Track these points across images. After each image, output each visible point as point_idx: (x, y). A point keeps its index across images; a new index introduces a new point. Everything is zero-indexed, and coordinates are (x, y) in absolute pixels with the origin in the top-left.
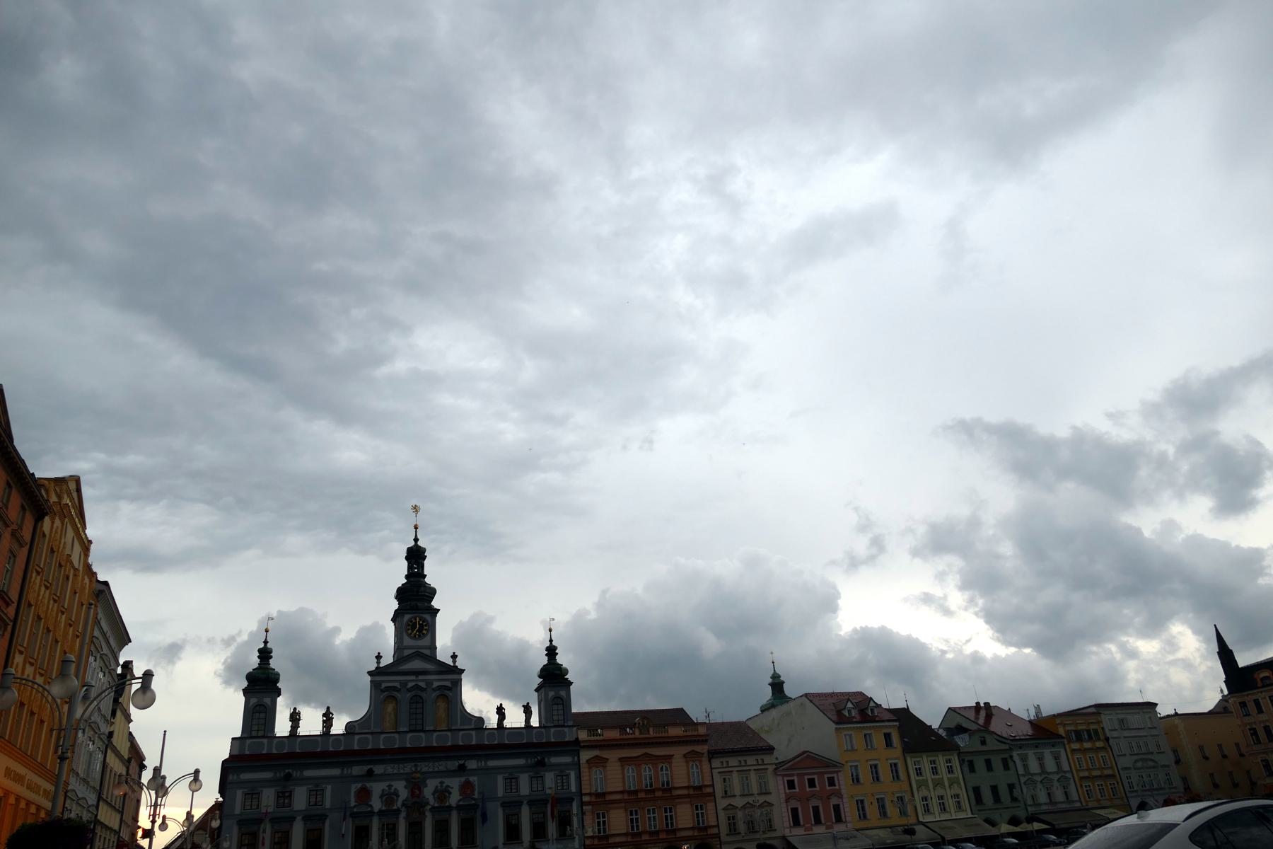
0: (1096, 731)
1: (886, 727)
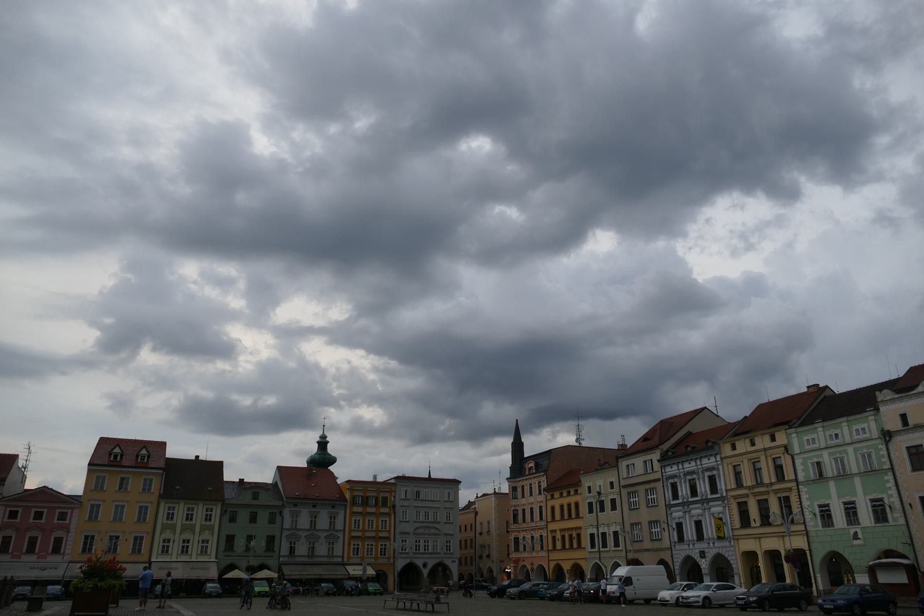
0: (385, 499)
1: (147, 474)
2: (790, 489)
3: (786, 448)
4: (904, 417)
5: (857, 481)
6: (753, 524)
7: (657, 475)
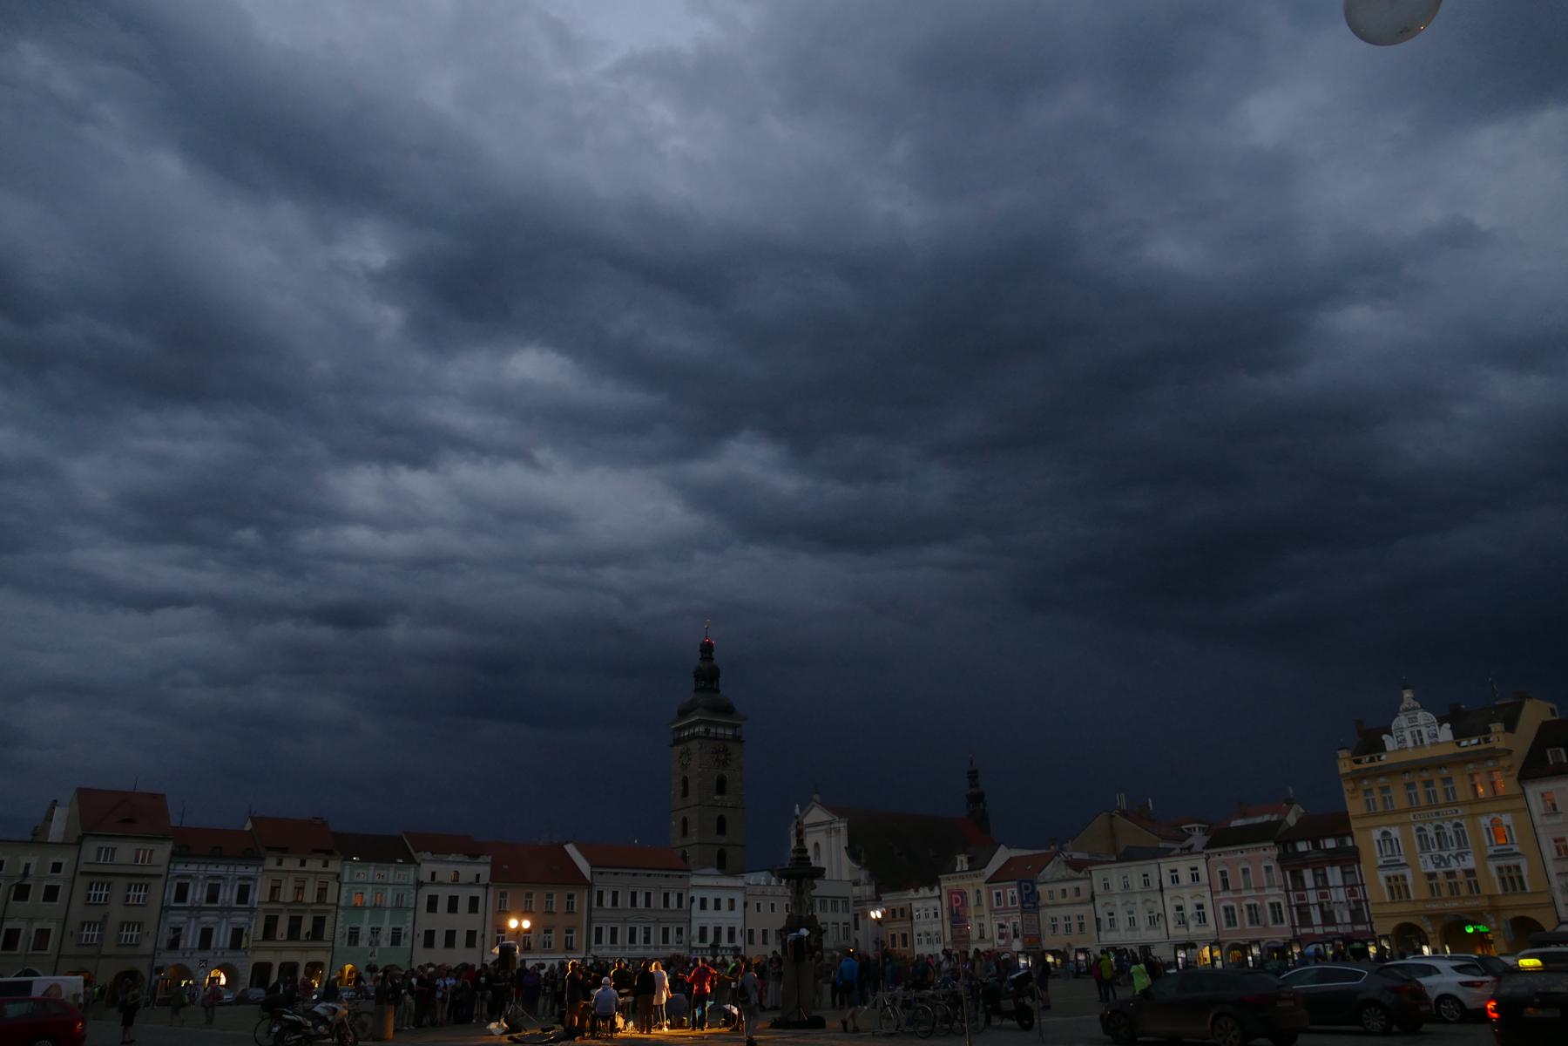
2: (328, 911)
3: (338, 876)
4: (433, 874)
5: (388, 913)
6: (278, 937)
7: (162, 870)
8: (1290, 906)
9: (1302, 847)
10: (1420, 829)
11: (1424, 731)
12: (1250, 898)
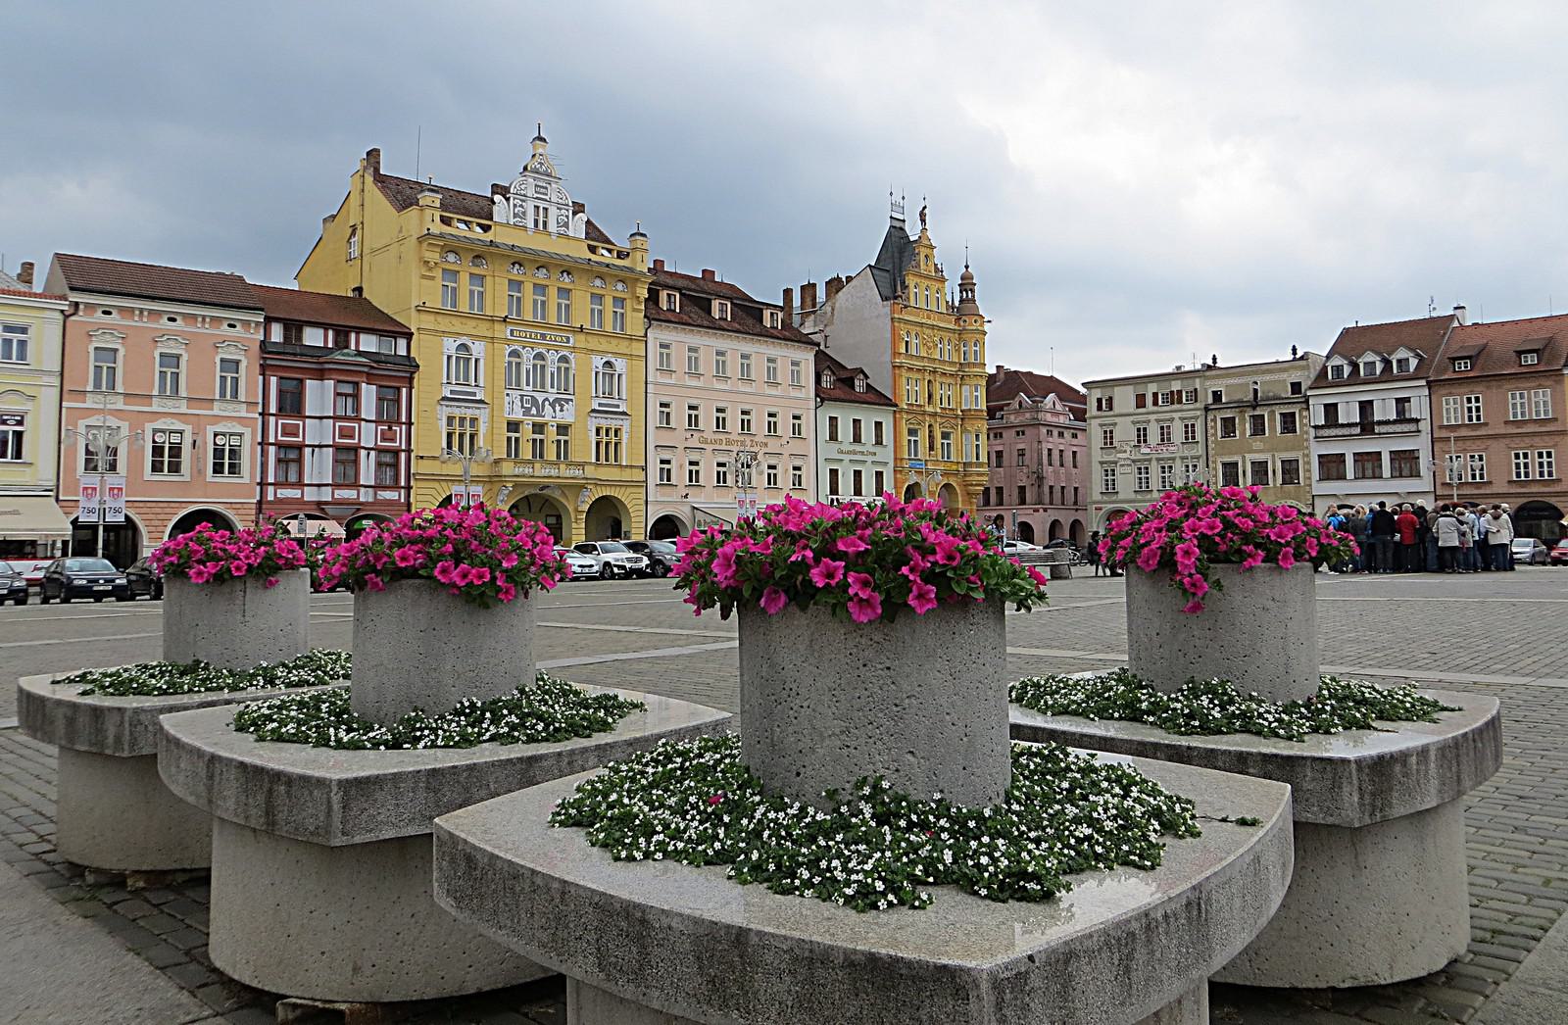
8: (264, 443)
9: (313, 337)
10: (515, 354)
11: (553, 211)
12: (169, 418)
